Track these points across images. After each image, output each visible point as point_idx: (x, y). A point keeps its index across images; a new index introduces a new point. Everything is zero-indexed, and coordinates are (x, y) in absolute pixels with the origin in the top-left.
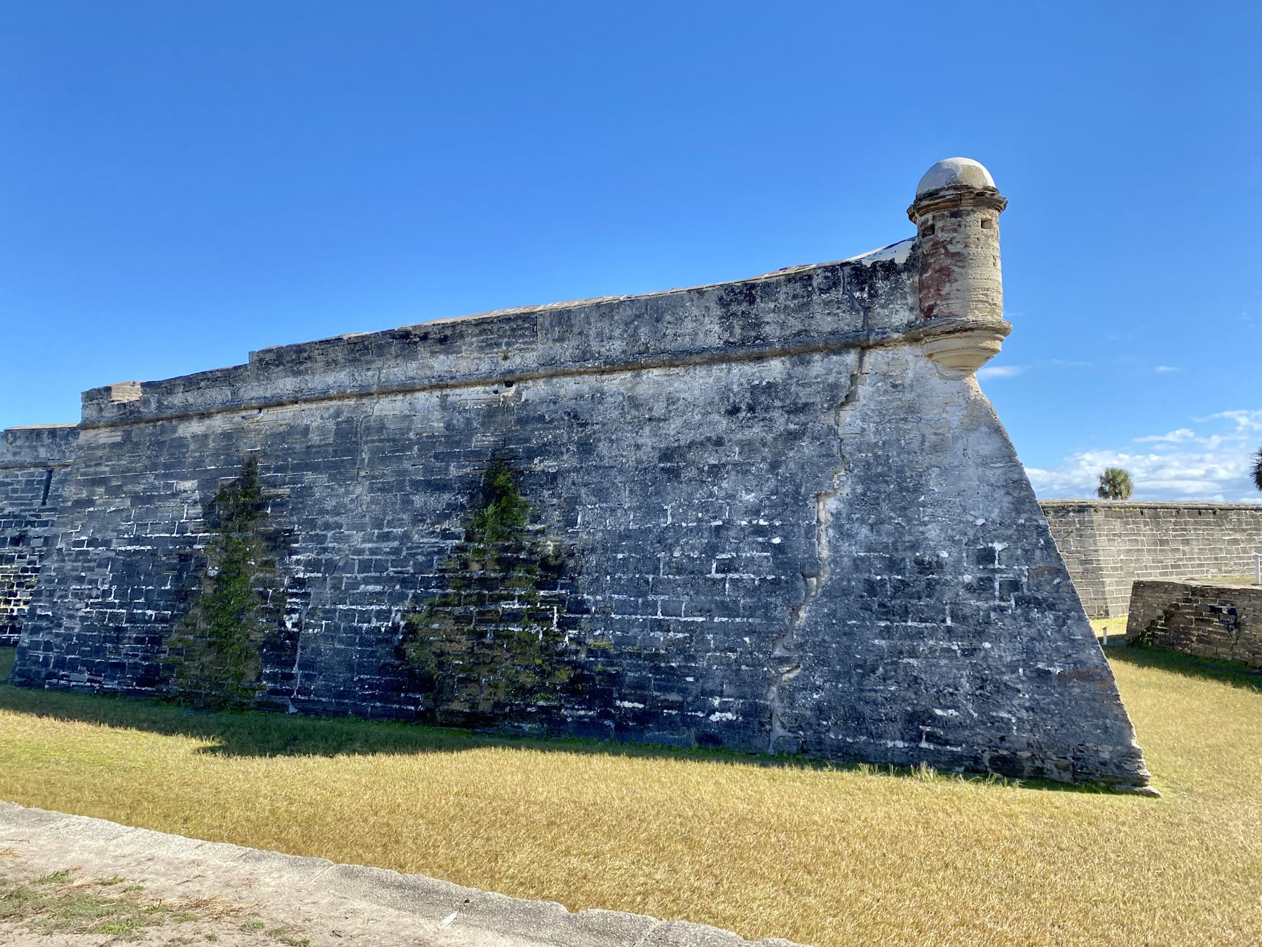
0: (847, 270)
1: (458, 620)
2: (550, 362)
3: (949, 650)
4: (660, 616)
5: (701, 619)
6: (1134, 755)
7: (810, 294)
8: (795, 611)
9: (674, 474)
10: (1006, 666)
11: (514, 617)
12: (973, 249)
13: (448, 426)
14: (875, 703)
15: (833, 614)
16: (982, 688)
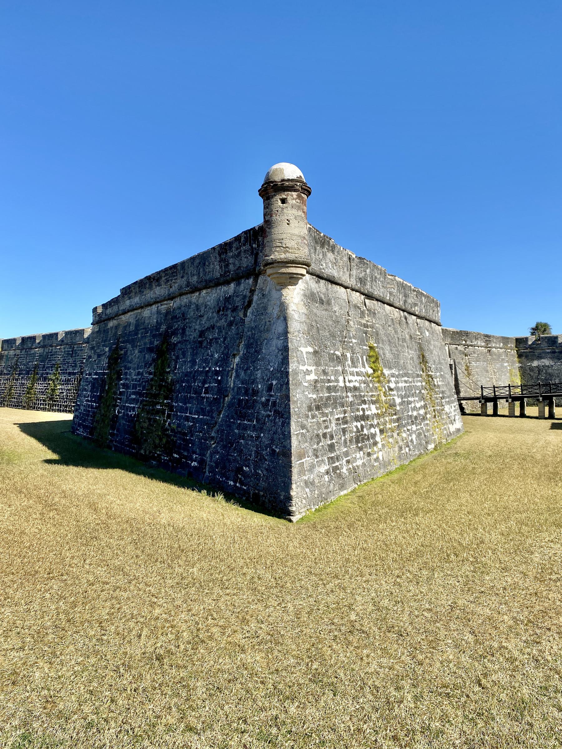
0: (252, 231)
1: (148, 413)
2: (181, 288)
3: (252, 437)
4: (188, 415)
5: (197, 416)
6: (289, 498)
7: (241, 246)
8: (219, 415)
9: (201, 343)
10: (265, 446)
11: (158, 412)
12: (274, 217)
13: (157, 322)
14: (229, 461)
15: (227, 416)
16: (257, 457)
